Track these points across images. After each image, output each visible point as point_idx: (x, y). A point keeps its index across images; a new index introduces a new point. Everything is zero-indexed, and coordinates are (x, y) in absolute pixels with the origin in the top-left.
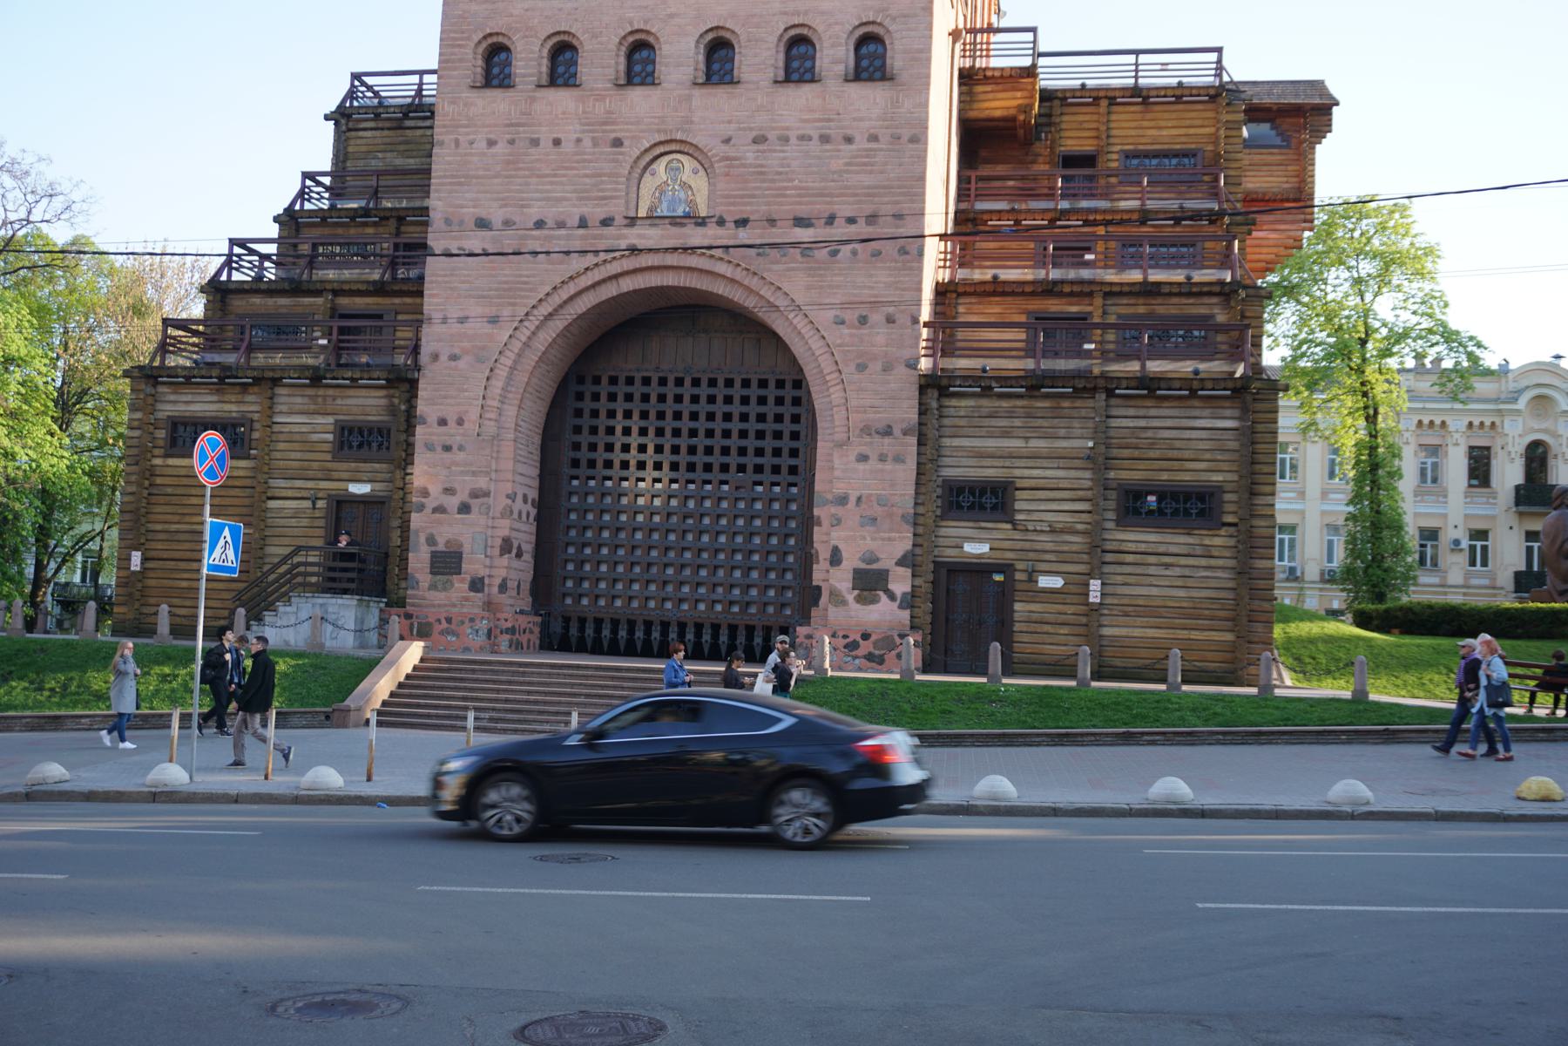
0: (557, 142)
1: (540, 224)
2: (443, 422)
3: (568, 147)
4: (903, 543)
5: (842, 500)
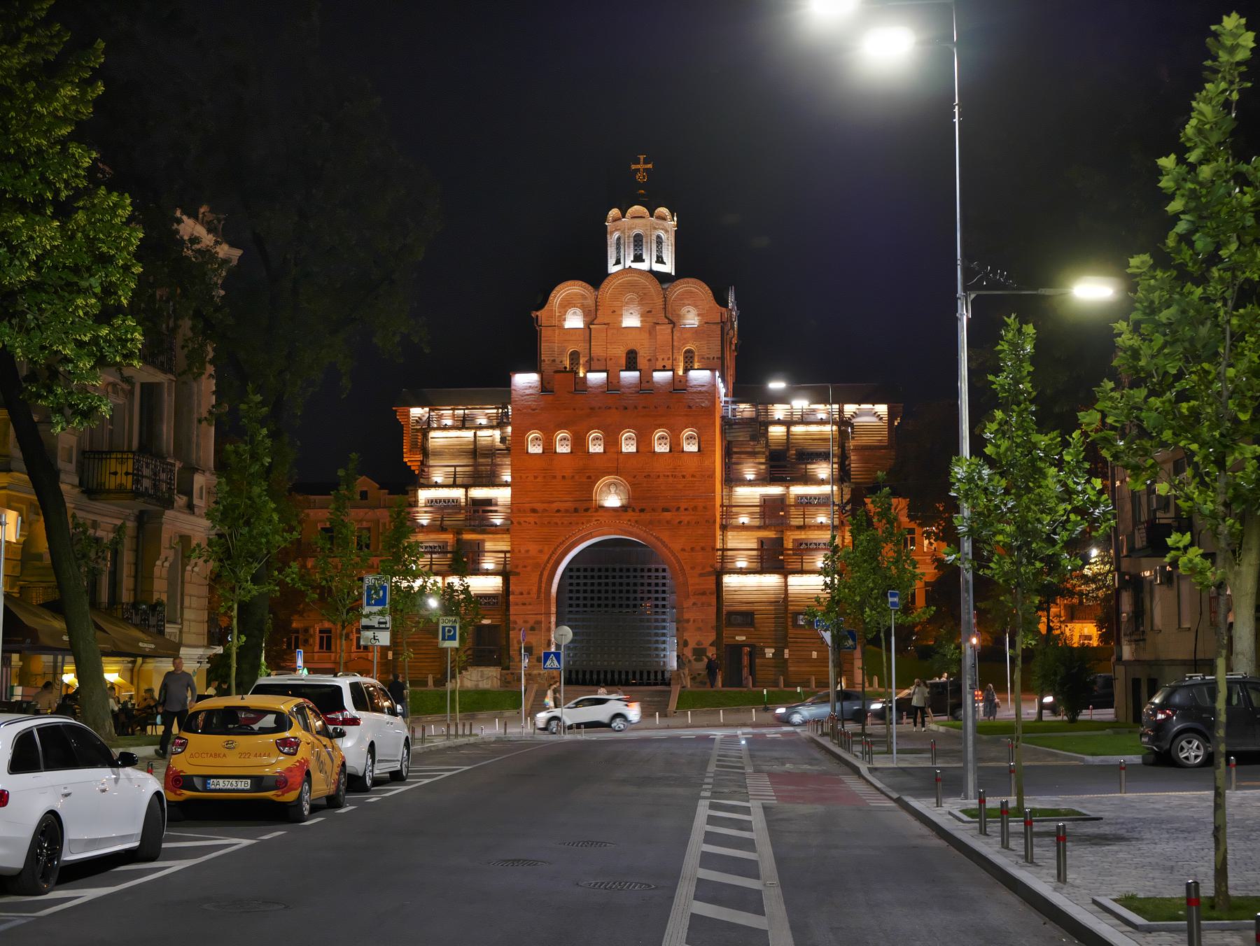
1: (558, 511)
4: (712, 637)
5: (688, 621)
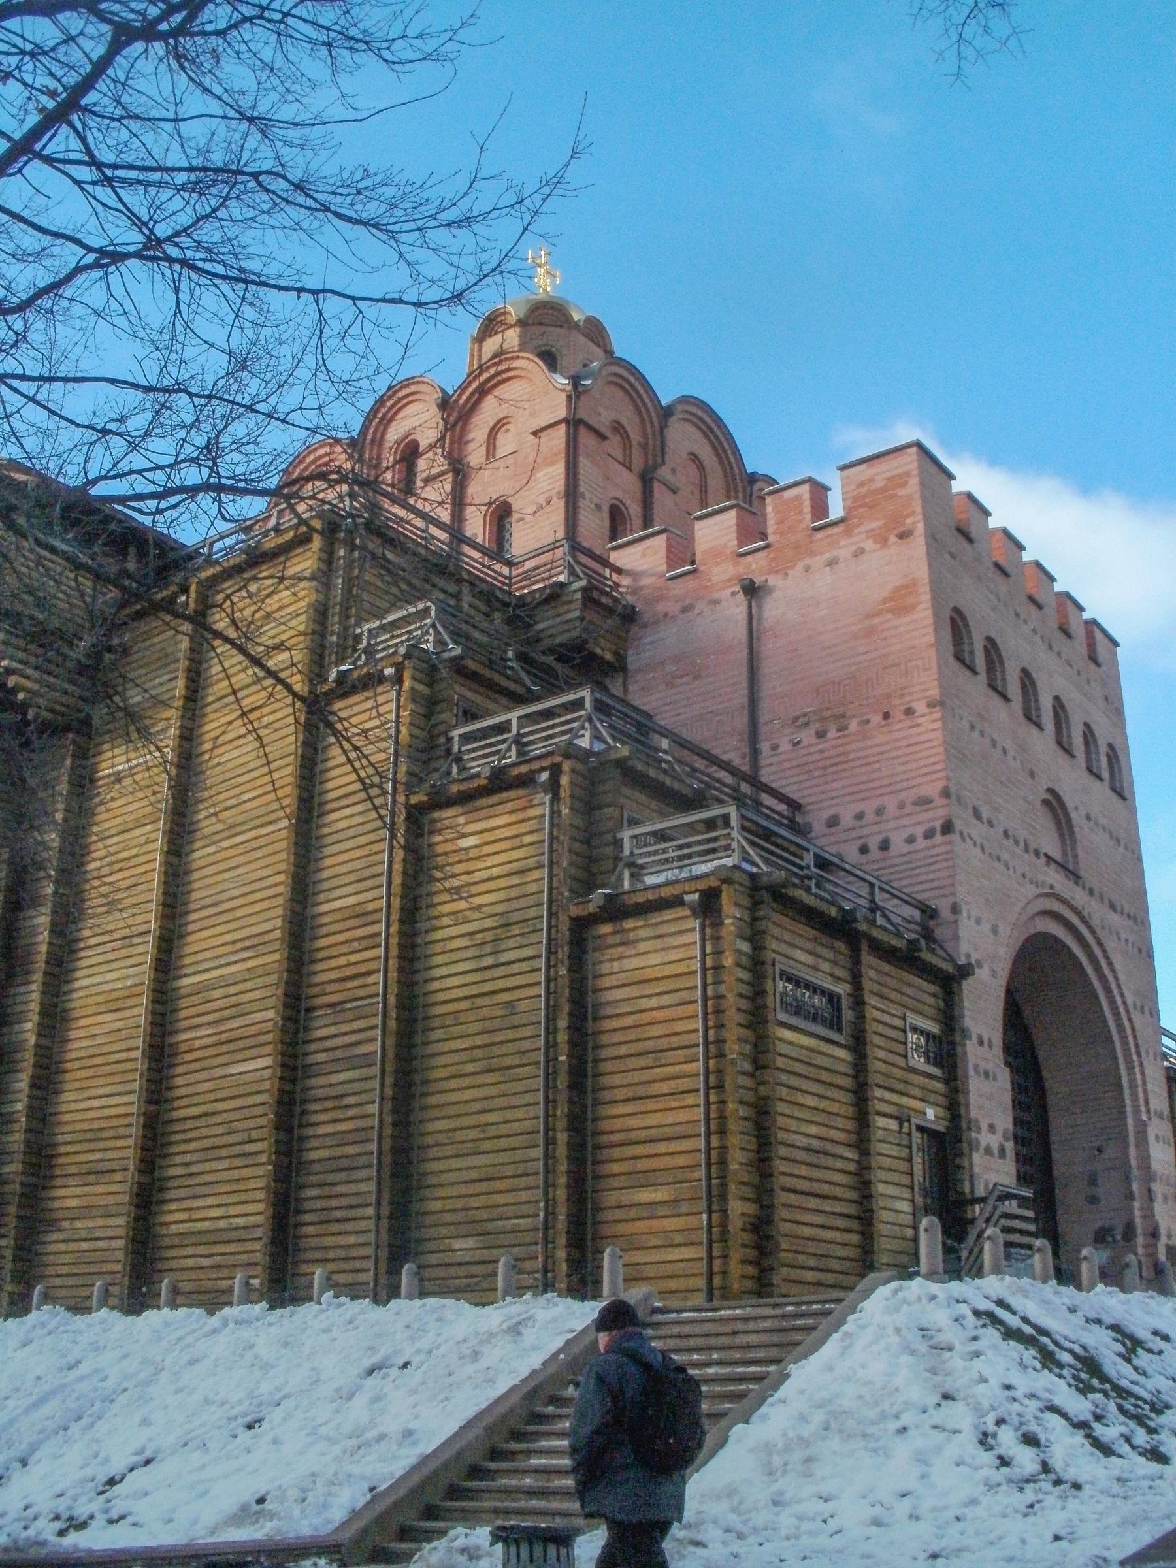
0: (1005, 751)
2: (981, 1043)
3: (1010, 758)
